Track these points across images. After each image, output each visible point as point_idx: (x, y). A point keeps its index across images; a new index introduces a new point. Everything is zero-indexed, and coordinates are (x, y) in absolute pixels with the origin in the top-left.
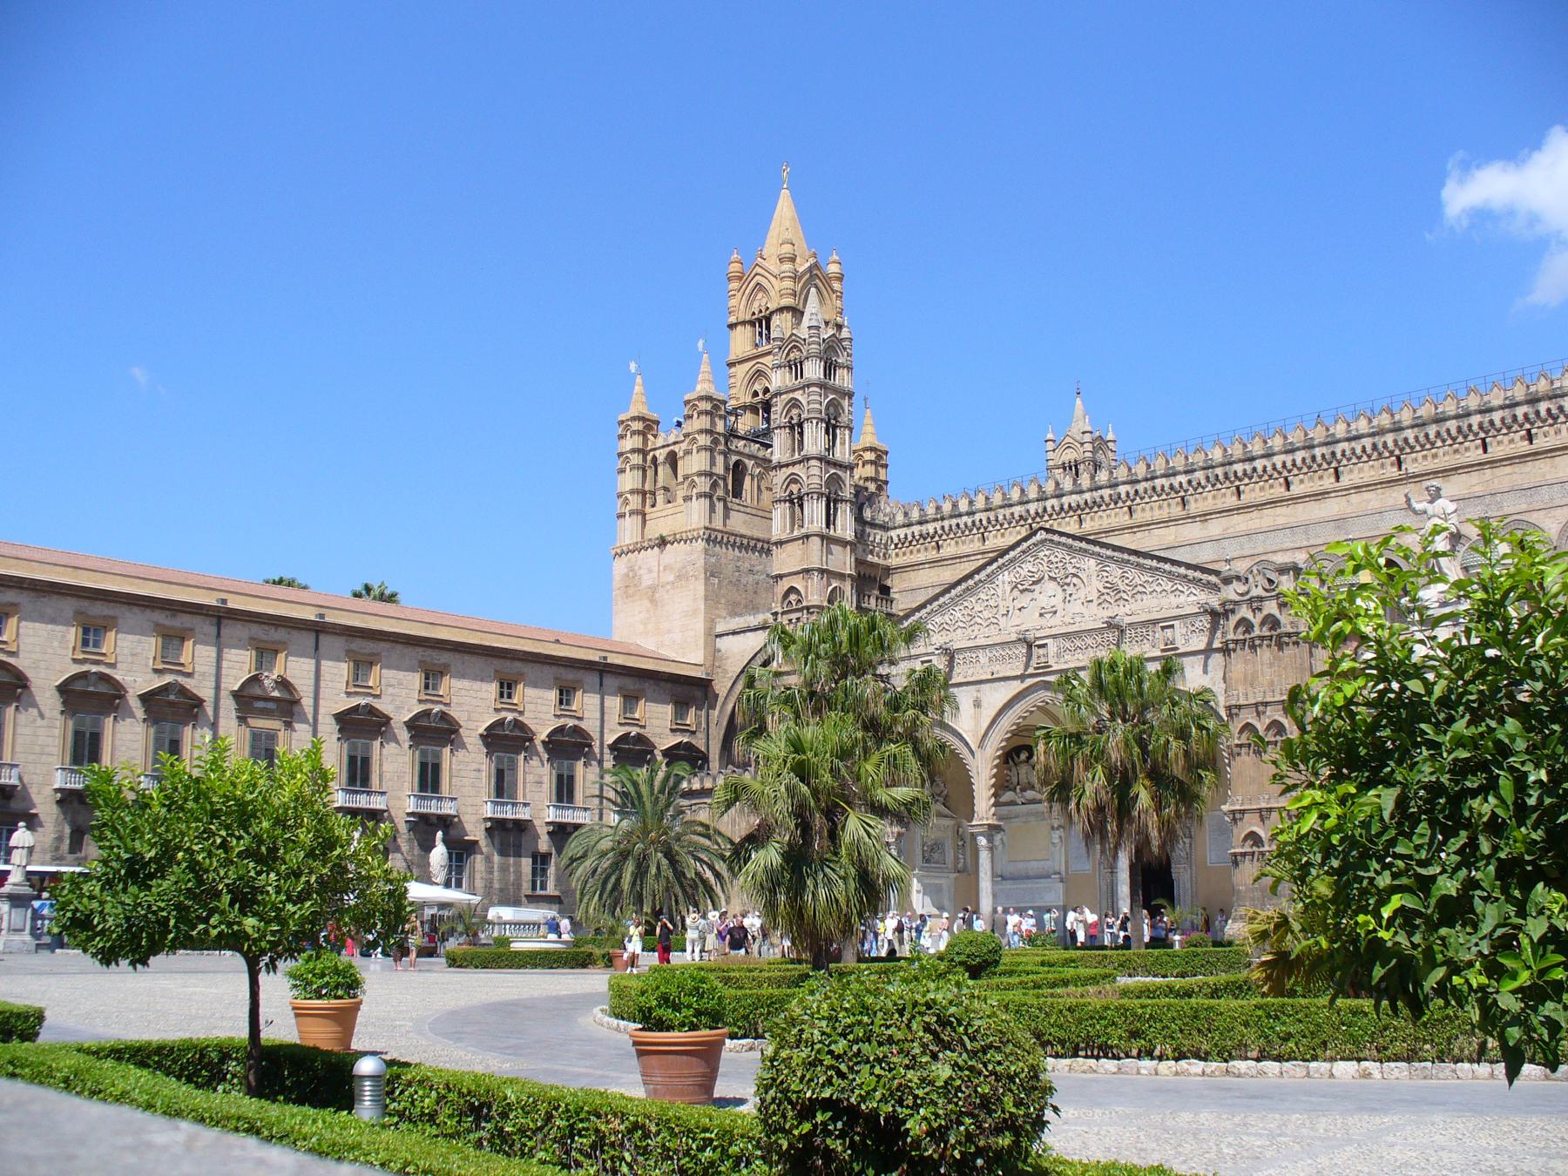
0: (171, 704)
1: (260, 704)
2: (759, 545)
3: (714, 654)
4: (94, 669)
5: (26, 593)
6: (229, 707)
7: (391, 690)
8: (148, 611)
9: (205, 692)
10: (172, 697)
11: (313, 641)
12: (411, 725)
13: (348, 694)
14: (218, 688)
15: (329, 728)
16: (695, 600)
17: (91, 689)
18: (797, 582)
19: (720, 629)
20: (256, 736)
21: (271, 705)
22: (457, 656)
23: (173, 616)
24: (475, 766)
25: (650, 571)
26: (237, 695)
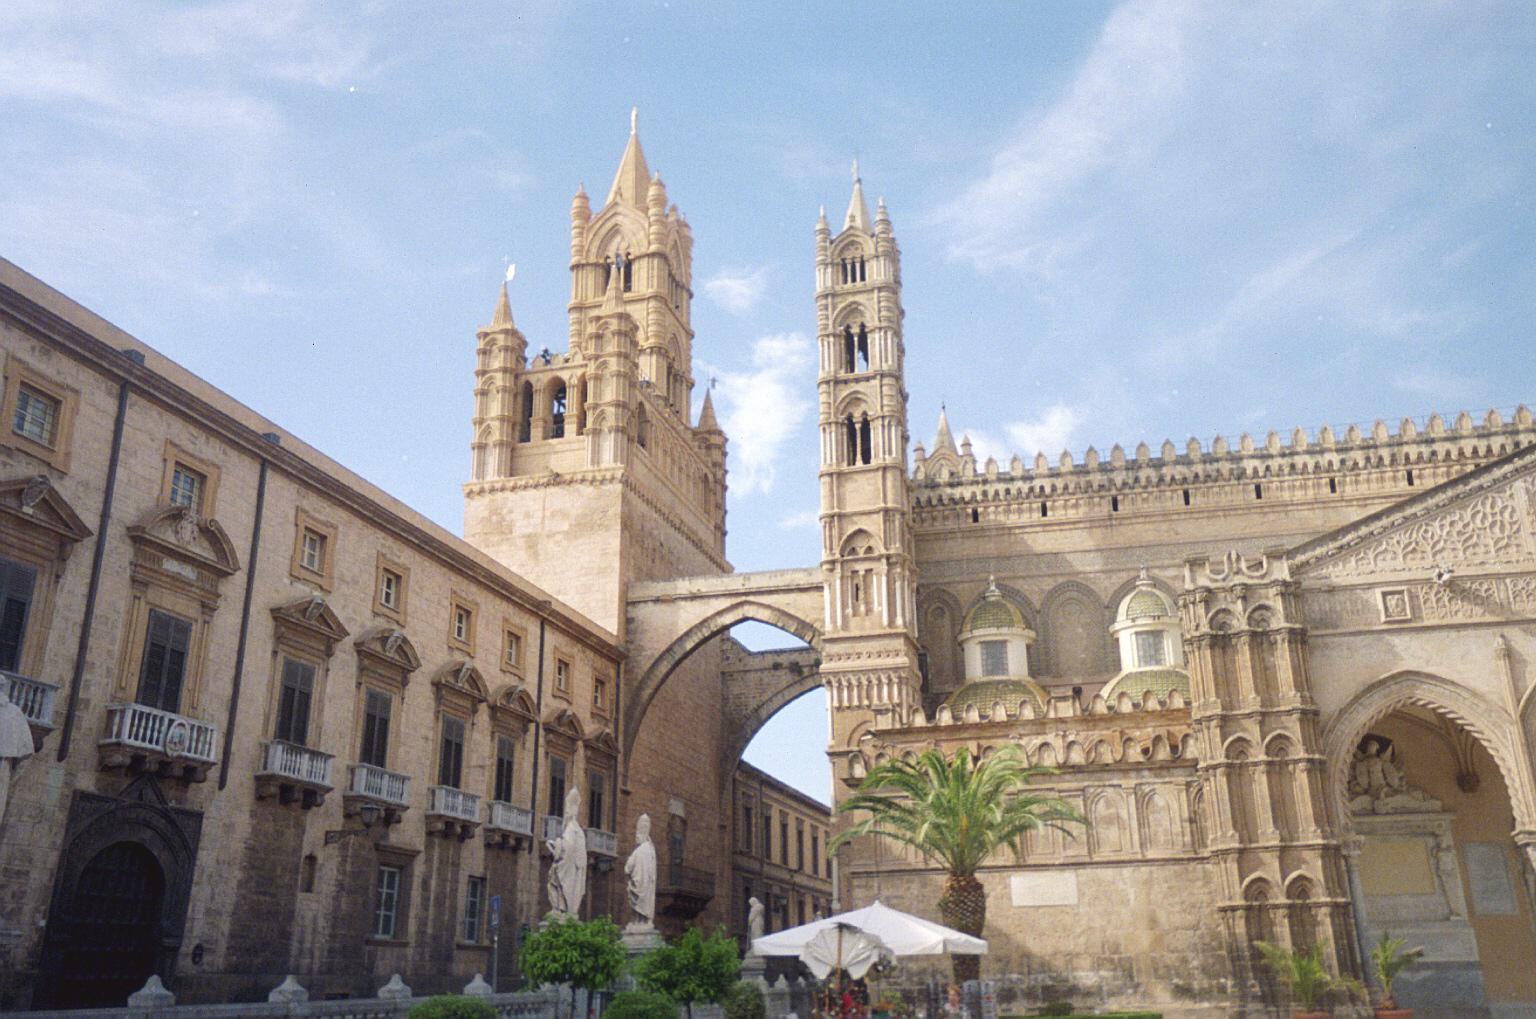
0: (24, 523)
1: (171, 566)
6: (119, 555)
7: (344, 588)
13: (295, 578)
14: (105, 516)
15: (262, 628)
16: (604, 554)
21: (188, 572)
23: (46, 353)
24: (424, 731)
25: (528, 515)
26: (137, 537)
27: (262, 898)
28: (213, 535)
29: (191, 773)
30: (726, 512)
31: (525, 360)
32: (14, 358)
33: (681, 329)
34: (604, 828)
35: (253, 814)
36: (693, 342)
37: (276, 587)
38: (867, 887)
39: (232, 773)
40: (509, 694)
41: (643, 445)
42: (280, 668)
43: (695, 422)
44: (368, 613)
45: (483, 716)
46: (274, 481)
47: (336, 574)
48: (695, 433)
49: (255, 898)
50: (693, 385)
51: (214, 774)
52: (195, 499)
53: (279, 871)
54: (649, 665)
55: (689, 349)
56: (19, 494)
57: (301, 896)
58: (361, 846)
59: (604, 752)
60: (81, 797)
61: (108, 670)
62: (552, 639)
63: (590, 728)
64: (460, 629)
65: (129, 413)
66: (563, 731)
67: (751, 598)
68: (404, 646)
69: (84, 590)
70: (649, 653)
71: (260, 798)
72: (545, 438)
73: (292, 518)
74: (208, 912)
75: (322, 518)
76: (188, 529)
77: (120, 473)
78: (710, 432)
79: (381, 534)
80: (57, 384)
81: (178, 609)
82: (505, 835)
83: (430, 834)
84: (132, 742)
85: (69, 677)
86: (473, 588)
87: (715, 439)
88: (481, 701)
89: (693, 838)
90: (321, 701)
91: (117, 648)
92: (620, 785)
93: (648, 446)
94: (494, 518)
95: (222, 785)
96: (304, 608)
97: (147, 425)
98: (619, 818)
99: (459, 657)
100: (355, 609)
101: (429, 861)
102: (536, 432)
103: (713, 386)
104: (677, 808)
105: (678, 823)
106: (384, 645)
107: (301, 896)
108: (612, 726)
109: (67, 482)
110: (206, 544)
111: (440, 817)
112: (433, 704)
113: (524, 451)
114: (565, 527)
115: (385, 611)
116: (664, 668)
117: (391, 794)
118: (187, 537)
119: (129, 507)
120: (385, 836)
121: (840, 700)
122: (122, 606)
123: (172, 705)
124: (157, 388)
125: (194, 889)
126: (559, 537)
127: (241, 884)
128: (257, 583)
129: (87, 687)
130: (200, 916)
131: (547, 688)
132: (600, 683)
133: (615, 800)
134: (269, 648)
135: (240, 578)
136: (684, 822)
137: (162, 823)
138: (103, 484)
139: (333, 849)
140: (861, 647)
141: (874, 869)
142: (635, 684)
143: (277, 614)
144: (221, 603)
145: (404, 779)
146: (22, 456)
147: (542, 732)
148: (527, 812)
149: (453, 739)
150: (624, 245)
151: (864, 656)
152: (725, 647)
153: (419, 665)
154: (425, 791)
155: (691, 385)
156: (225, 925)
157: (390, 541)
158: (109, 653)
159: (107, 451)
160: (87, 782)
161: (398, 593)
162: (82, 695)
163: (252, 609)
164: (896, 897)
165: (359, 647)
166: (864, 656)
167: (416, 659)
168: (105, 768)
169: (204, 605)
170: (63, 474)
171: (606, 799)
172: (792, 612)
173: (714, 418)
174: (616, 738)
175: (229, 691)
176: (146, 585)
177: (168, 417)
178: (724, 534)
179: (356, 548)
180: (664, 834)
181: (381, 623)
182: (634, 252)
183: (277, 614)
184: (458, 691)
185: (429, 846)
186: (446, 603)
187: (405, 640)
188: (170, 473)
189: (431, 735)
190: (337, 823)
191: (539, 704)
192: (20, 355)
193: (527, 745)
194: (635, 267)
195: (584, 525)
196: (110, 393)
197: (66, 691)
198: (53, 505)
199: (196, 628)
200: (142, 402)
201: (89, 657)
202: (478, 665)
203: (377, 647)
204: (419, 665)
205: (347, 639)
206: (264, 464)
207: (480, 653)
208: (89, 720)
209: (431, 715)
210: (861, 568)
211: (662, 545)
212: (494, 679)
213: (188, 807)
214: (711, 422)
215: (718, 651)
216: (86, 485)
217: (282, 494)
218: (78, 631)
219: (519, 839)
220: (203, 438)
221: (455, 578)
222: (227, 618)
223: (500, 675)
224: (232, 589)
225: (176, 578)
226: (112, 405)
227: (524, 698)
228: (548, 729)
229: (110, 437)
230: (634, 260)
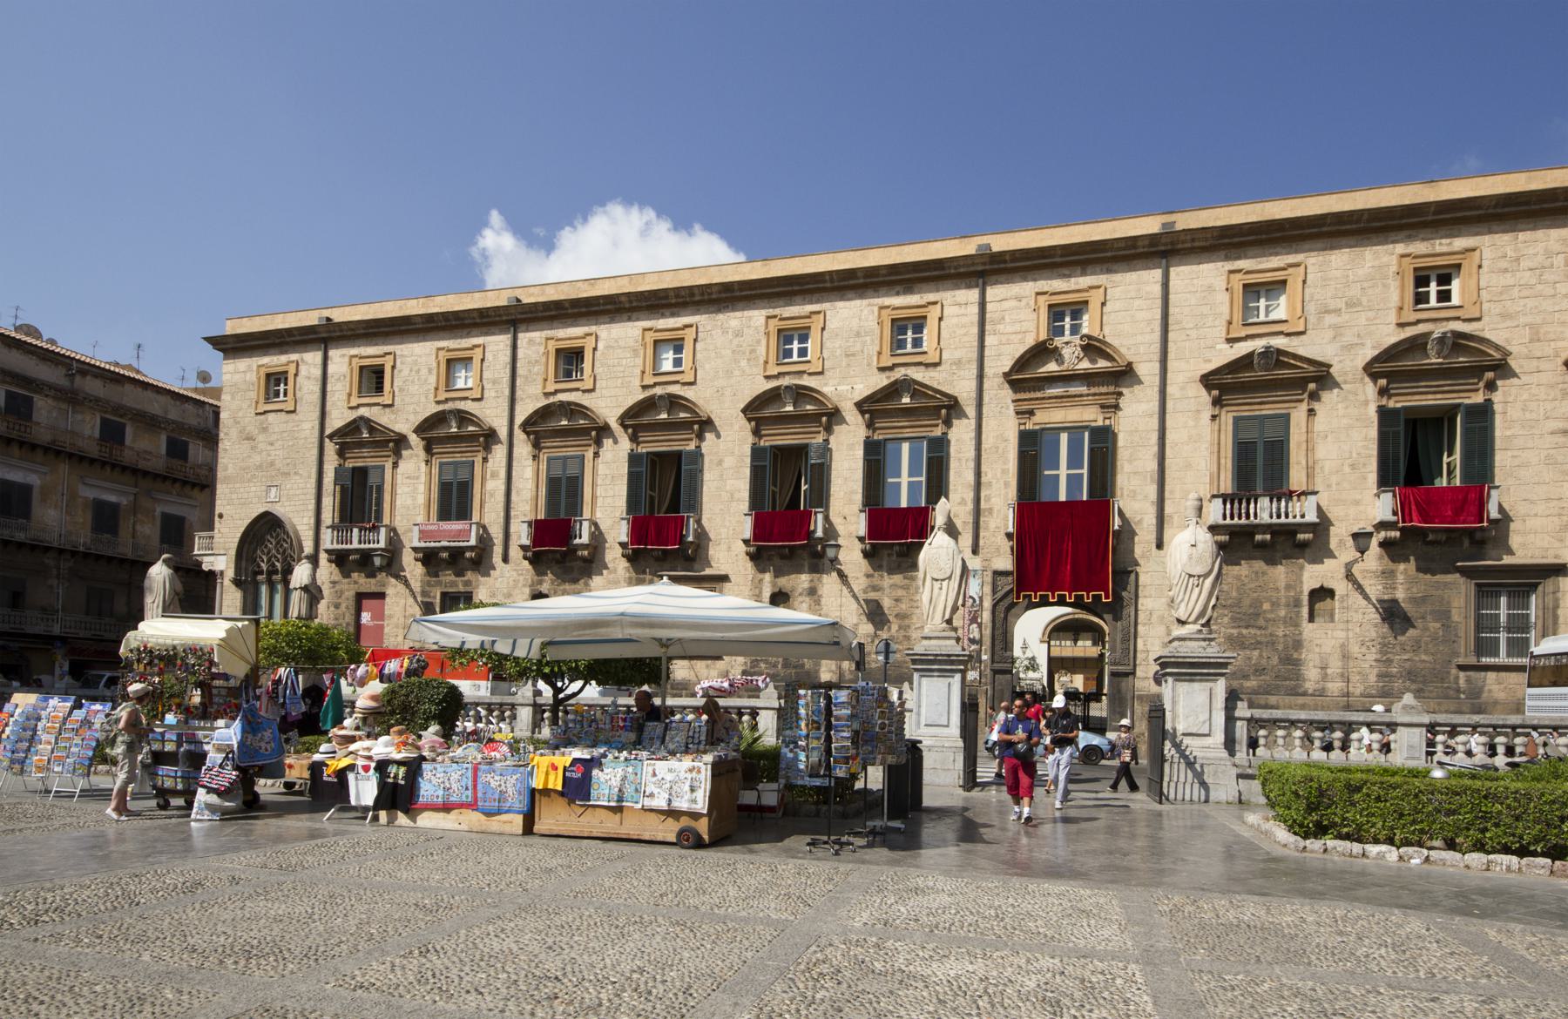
0: (907, 412)
6: (1000, 400)
9: (962, 387)
15: (1190, 402)
27: (1244, 631)
49: (1235, 631)
53: (1266, 606)
57: (1308, 629)
60: (997, 573)
77: (989, 340)
95: (1160, 546)
107: (1308, 629)
128: (1171, 365)
129: (988, 499)
159: (975, 330)
162: (983, 505)
163: (1169, 389)
176: (1031, 413)
218: (972, 464)
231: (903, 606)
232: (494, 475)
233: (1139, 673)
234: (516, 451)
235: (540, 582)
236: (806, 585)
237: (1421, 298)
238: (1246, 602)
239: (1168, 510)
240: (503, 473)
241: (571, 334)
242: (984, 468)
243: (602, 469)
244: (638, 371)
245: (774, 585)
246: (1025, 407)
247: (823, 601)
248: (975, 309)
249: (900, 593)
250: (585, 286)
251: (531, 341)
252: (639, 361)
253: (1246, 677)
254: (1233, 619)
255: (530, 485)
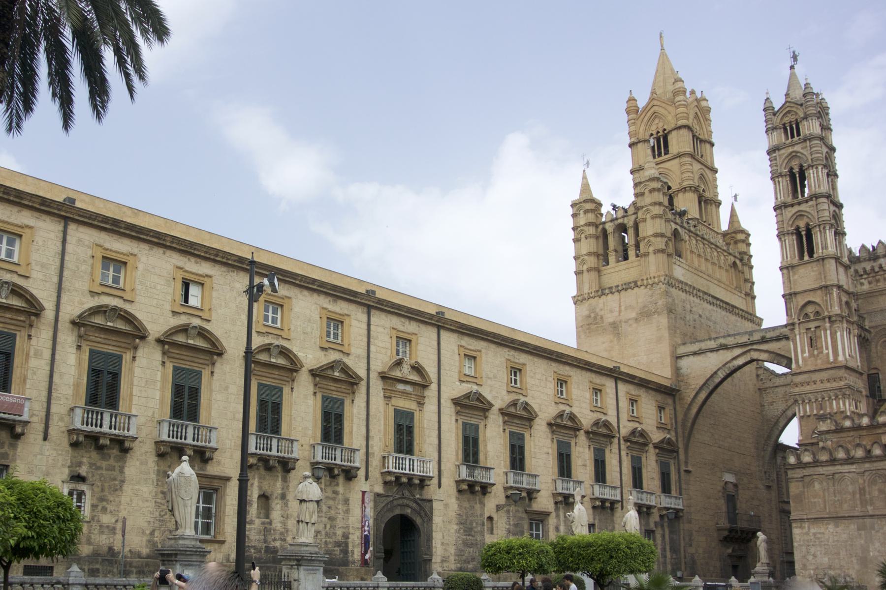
0: (336, 380)
1: (401, 387)
2: (695, 292)
3: (677, 370)
4: (276, 343)
5: (217, 267)
6: (377, 387)
7: (489, 382)
8: (315, 295)
10: (336, 374)
11: (435, 336)
12: (503, 412)
14: (368, 369)
15: (448, 410)
16: (659, 329)
17: (273, 360)
18: (817, 297)
19: (682, 350)
20: (398, 413)
21: (409, 388)
22: (530, 357)
23: (335, 301)
24: (546, 450)
26: (384, 377)
28: (417, 369)
29: (423, 481)
30: (753, 283)
31: (602, 215)
32: (323, 308)
33: (706, 169)
34: (674, 493)
35: (458, 499)
36: (717, 175)
37: (454, 388)
38: (801, 527)
39: (443, 480)
40: (596, 423)
41: (680, 256)
42: (461, 427)
43: (724, 226)
44: (505, 392)
45: (582, 437)
46: (444, 335)
47: (484, 376)
48: (725, 235)
50: (720, 204)
51: (435, 481)
52: (408, 352)
53: (474, 525)
54: (692, 396)
55: (715, 180)
56: (332, 367)
58: (517, 511)
59: (666, 449)
60: (378, 495)
61: (380, 439)
62: (622, 387)
63: (656, 436)
64: (562, 391)
65: (372, 319)
66: (637, 441)
67: (755, 347)
68: (526, 407)
69: (365, 404)
70: (693, 387)
71: (460, 491)
72: (618, 261)
73: (456, 352)
74: (442, 544)
75: (472, 348)
76: (406, 368)
77: (372, 348)
78: (735, 232)
79: (506, 350)
80: (340, 315)
81: (406, 406)
82: (603, 501)
83: (556, 503)
84: (394, 470)
85: (364, 443)
86: (567, 368)
87: (741, 237)
88: (579, 430)
89: (743, 496)
90: (485, 441)
91: (382, 428)
92: (683, 468)
93: (684, 255)
94: (593, 315)
95: (440, 487)
96: (468, 396)
97: (383, 323)
98: (683, 486)
99: (562, 407)
100: (497, 394)
101: (558, 516)
102: (612, 258)
103: (736, 200)
104: (729, 478)
105: (730, 487)
106: (516, 408)
108: (673, 433)
109: (350, 357)
110: (415, 373)
111: (560, 494)
112: (550, 435)
113: (605, 272)
114: (633, 315)
115: (515, 390)
116: (703, 395)
117: (528, 484)
118: (405, 372)
119: (382, 360)
120: (530, 506)
121: (805, 411)
122: (382, 409)
123: (410, 451)
124: (382, 305)
125: (434, 534)
126: (630, 322)
127: (457, 531)
128: (442, 387)
129: (372, 448)
130: (439, 545)
131: (624, 416)
132: (661, 408)
133: (680, 477)
134: (454, 418)
135: (434, 386)
136: (735, 486)
137: (414, 505)
138: (365, 355)
139: (502, 513)
140: (816, 376)
141: (805, 517)
142: (686, 406)
143: (456, 402)
144: (426, 400)
145: (536, 476)
146: (332, 351)
147: (622, 442)
148: (616, 488)
149: (565, 452)
150: (661, 125)
151: (818, 382)
152: (759, 373)
153: (537, 416)
154: (550, 481)
155: (719, 204)
156: (452, 550)
157: (512, 352)
158: (379, 431)
159: (365, 339)
160: (379, 489)
161: (521, 378)
163: (442, 401)
164: (820, 533)
165: (503, 412)
166: (818, 382)
167: (535, 412)
168: (386, 483)
169: (419, 403)
170: (348, 354)
171: (674, 477)
172: (782, 353)
173: (739, 222)
174: (677, 441)
175: (436, 442)
176: (390, 398)
177: (390, 317)
178: (754, 298)
179: (494, 361)
180: (720, 494)
181: (513, 397)
182: (668, 128)
183: (456, 402)
184: (564, 426)
185: (557, 509)
186: (551, 379)
187: (527, 403)
188: (394, 343)
189: (550, 451)
190: (502, 500)
191: (618, 427)
192: (325, 306)
193: (613, 450)
194: (669, 138)
195: (645, 314)
196: (363, 312)
197: (363, 450)
198: (345, 370)
199: (417, 415)
200: (377, 312)
201: (371, 434)
202: (575, 410)
203: (512, 410)
204: (537, 416)
205: (494, 408)
206: (439, 328)
207: (575, 404)
208: (375, 462)
209: (549, 441)
210: (812, 325)
211: (700, 316)
212: (586, 418)
213: (425, 497)
214: (736, 225)
215: (754, 376)
216: (358, 357)
217: (450, 341)
219: (613, 503)
220: (407, 322)
221: (554, 364)
222: (430, 407)
223: (592, 414)
224: (431, 392)
225: (404, 393)
226: (364, 317)
227: (607, 424)
228: (626, 440)
229: (366, 332)
230: (670, 132)
231: (333, 512)
232: (38, 354)
233: (433, 560)
234: (61, 337)
235: (80, 464)
236: (279, 491)
237: (328, 335)
238: (468, 522)
239: (443, 468)
240: (47, 354)
241: (120, 246)
242: (371, 427)
243: (137, 371)
244: (169, 298)
245: (260, 488)
246: (388, 394)
247: (290, 504)
248: (365, 326)
249: (331, 503)
250: (129, 212)
251: (80, 240)
252: (171, 290)
253: (469, 562)
254: (465, 531)
255: (73, 371)
